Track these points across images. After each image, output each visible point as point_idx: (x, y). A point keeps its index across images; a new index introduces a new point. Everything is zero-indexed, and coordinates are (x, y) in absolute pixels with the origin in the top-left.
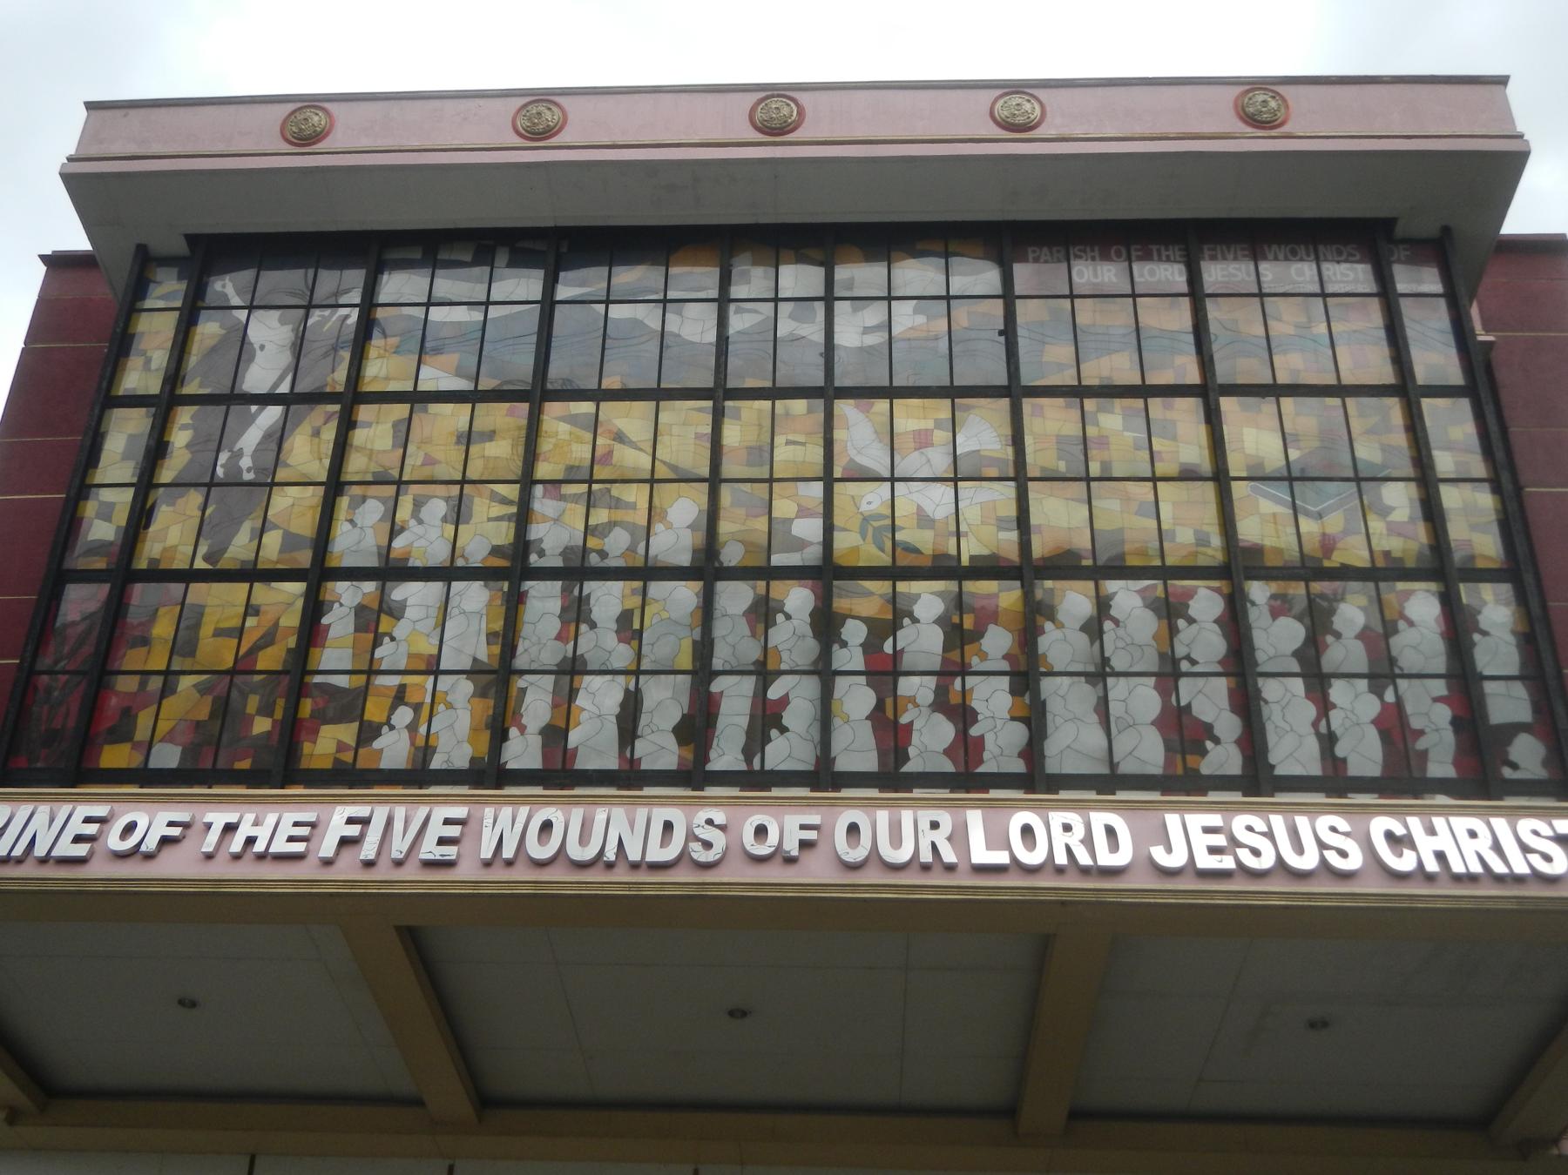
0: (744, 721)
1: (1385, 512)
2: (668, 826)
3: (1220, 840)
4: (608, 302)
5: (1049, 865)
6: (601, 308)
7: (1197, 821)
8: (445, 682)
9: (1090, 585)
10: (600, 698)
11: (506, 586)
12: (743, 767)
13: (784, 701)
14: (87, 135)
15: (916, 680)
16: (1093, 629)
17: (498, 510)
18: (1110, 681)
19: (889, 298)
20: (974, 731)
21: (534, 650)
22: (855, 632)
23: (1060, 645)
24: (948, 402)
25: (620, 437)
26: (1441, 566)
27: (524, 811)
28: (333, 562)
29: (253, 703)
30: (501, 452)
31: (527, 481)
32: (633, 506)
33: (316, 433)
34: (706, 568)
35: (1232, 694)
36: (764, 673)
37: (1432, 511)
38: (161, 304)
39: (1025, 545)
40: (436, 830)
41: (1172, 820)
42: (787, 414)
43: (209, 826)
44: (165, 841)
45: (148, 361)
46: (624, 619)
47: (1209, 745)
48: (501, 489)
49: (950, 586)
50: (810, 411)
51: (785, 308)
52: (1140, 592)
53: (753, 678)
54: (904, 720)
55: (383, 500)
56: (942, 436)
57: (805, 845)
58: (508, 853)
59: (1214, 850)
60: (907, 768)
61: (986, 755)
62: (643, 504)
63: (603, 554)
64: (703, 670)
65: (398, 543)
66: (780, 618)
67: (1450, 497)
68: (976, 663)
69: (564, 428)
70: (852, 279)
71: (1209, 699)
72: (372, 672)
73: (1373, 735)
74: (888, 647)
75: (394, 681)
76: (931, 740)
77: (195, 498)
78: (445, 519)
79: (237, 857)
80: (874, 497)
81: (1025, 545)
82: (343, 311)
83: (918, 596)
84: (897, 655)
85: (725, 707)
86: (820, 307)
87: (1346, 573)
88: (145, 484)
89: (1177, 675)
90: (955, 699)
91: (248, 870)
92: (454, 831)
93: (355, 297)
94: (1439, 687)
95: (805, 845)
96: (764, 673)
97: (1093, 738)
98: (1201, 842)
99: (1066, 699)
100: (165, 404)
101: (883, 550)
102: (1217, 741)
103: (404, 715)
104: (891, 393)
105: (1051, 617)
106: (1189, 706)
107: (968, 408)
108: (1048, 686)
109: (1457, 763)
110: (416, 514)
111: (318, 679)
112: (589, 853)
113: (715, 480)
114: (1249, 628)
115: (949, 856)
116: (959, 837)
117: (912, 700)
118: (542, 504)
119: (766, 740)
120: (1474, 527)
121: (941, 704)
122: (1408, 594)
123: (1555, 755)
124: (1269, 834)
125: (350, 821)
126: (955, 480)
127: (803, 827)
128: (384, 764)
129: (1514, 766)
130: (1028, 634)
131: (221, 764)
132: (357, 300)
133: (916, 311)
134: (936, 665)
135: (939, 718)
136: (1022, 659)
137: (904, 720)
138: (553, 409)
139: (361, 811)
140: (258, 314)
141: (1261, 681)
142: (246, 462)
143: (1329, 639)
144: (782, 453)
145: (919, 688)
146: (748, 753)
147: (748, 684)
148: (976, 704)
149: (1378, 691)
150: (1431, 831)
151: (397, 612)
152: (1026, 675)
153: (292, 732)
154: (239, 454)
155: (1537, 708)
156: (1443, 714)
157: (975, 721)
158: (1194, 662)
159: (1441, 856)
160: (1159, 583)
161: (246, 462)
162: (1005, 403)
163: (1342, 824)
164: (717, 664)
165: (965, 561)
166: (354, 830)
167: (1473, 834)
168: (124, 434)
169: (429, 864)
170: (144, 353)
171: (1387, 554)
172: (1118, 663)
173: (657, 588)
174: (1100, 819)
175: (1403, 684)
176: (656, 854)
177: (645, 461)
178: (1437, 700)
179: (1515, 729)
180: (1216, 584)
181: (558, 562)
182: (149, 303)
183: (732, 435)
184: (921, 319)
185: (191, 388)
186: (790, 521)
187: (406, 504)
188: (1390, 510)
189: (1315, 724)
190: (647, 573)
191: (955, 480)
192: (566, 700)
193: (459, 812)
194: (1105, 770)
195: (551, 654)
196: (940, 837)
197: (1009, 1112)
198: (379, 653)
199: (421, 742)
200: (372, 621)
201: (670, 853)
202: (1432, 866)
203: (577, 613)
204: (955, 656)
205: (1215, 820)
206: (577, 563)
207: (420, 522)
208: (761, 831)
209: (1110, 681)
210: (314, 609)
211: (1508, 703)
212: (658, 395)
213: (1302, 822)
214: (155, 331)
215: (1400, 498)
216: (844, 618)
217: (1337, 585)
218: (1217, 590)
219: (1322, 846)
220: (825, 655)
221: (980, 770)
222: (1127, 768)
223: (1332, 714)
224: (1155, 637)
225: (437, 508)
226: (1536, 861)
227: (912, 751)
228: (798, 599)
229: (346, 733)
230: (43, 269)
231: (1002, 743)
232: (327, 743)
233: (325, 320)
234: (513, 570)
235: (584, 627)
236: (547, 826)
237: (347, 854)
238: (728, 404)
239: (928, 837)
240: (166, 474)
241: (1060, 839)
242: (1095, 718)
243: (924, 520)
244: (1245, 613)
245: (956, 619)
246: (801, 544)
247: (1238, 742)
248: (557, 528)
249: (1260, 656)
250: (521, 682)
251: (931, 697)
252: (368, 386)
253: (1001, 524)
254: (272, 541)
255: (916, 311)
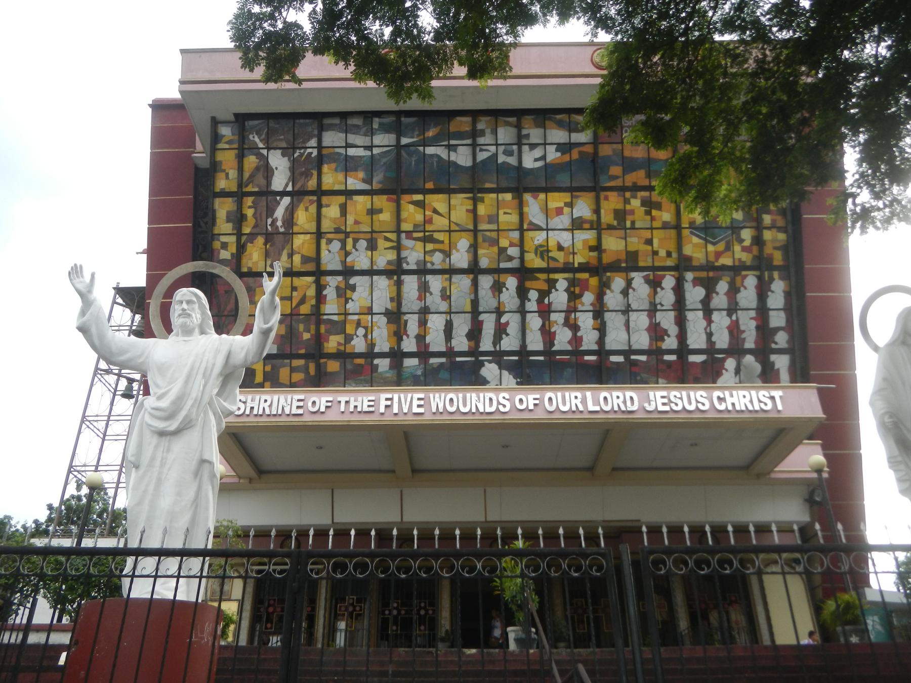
0: (492, 332)
1: (741, 241)
2: (491, 399)
3: (665, 401)
4: (424, 146)
5: (613, 411)
6: (421, 148)
7: (659, 394)
8: (376, 318)
9: (624, 274)
10: (436, 323)
11: (395, 278)
12: (493, 349)
13: (507, 323)
14: (185, 68)
15: (557, 314)
16: (625, 293)
17: (389, 244)
18: (631, 313)
19: (545, 144)
20: (579, 334)
21: (409, 305)
22: (533, 295)
23: (613, 299)
24: (569, 194)
25: (435, 211)
26: (762, 265)
27: (443, 395)
28: (323, 268)
29: (301, 327)
30: (386, 217)
31: (398, 231)
32: (442, 242)
33: (307, 209)
34: (474, 270)
35: (676, 317)
36: (499, 312)
37: (758, 241)
38: (227, 146)
39: (600, 259)
40: (416, 403)
41: (651, 394)
42: (503, 200)
43: (340, 402)
44: (327, 407)
45: (227, 175)
46: (443, 290)
47: (666, 337)
48: (388, 235)
49: (570, 275)
50: (513, 198)
51: (501, 149)
52: (644, 277)
53: (494, 315)
54: (553, 330)
55: (340, 240)
56: (567, 210)
57: (535, 405)
58: (441, 410)
59: (664, 404)
60: (553, 349)
61: (583, 343)
62: (447, 241)
63: (433, 264)
64: (475, 312)
65: (348, 260)
66: (504, 289)
67: (767, 235)
68: (580, 307)
69: (411, 207)
70: (529, 135)
71: (667, 320)
72: (346, 314)
73: (726, 333)
74: (546, 301)
75: (356, 317)
76: (562, 339)
77: (260, 240)
78: (367, 249)
79: (352, 412)
80: (539, 238)
81: (600, 259)
82: (309, 150)
83: (557, 280)
84: (550, 304)
85: (485, 326)
86: (515, 147)
87: (724, 268)
88: (239, 234)
89: (656, 310)
90: (572, 322)
91: (356, 418)
92: (422, 402)
93: (313, 142)
94: (753, 314)
95: (535, 405)
96: (499, 312)
97: (623, 335)
98: (660, 401)
99: (614, 321)
100: (239, 195)
101: (543, 260)
102: (669, 336)
103: (361, 331)
104: (546, 190)
105: (609, 288)
106: (659, 323)
107: (577, 197)
108: (607, 316)
109: (756, 342)
110: (354, 246)
111: (325, 317)
112: (466, 410)
113: (475, 231)
114: (684, 291)
115: (581, 408)
116: (584, 401)
117: (556, 322)
118: (406, 242)
119: (501, 339)
120: (775, 248)
121: (567, 323)
122: (745, 277)
123: (791, 341)
124: (681, 398)
125: (387, 399)
126: (572, 230)
127: (535, 399)
128: (357, 351)
129: (776, 343)
130: (600, 296)
131: (294, 352)
132: (315, 145)
133: (557, 150)
134: (564, 308)
135: (566, 329)
136: (598, 305)
137: (553, 330)
138: (406, 198)
139: (390, 396)
140: (272, 151)
141: (687, 313)
142: (279, 223)
143: (714, 295)
144: (502, 218)
145: (557, 318)
146: (494, 344)
147: (494, 315)
148: (580, 323)
149: (729, 315)
150: (732, 396)
151: (353, 288)
152: (599, 312)
153: (319, 340)
154: (276, 219)
155: (788, 321)
156: (753, 324)
157: (579, 330)
158: (662, 305)
159: (733, 404)
160: (651, 273)
161: (279, 223)
162: (592, 195)
163: (704, 394)
164: (481, 309)
165: (576, 265)
166: (389, 403)
167: (744, 397)
168: (223, 208)
169: (416, 414)
170: (224, 171)
171: (740, 260)
172: (634, 306)
173: (456, 278)
174: (629, 394)
175: (739, 312)
176: (488, 410)
177: (446, 222)
178: (751, 318)
179: (777, 329)
180: (673, 273)
181: (414, 267)
182: (220, 146)
183: (482, 210)
184: (559, 154)
185: (250, 188)
186: (505, 249)
187: (350, 241)
188: (743, 241)
189: (705, 329)
190: (451, 271)
191: (572, 230)
192: (423, 323)
193: (422, 396)
194: (627, 348)
195: (417, 306)
196: (578, 402)
197: (591, 469)
198: (348, 306)
199: (369, 342)
200: (343, 293)
201: (493, 409)
202: (730, 408)
203: (424, 288)
204: (572, 304)
205: (664, 393)
206: (422, 267)
207: (357, 250)
208: (521, 401)
209: (631, 313)
210: (320, 288)
211: (777, 319)
212: (449, 191)
213: (692, 393)
214: (227, 158)
215: (747, 235)
216: (530, 289)
217: (720, 273)
218: (673, 276)
219: (697, 402)
220: (522, 305)
221: (581, 349)
222: (634, 347)
223: (713, 325)
224: (649, 296)
225: (363, 244)
226: (763, 406)
227: (556, 342)
228: (512, 282)
229: (340, 338)
230: (149, 111)
231: (589, 339)
232: (333, 343)
233: (301, 155)
234: (396, 272)
235: (428, 294)
236: (451, 400)
237: (388, 409)
238: (479, 195)
239: (574, 401)
240: (247, 230)
241: (616, 401)
242: (624, 328)
243: (560, 248)
244: (683, 285)
245: (572, 289)
246: (510, 259)
247: (677, 336)
248: (413, 254)
249: (687, 303)
250: (406, 317)
251: (563, 321)
252: (324, 188)
253: (592, 249)
254: (297, 259)
255: (557, 150)
